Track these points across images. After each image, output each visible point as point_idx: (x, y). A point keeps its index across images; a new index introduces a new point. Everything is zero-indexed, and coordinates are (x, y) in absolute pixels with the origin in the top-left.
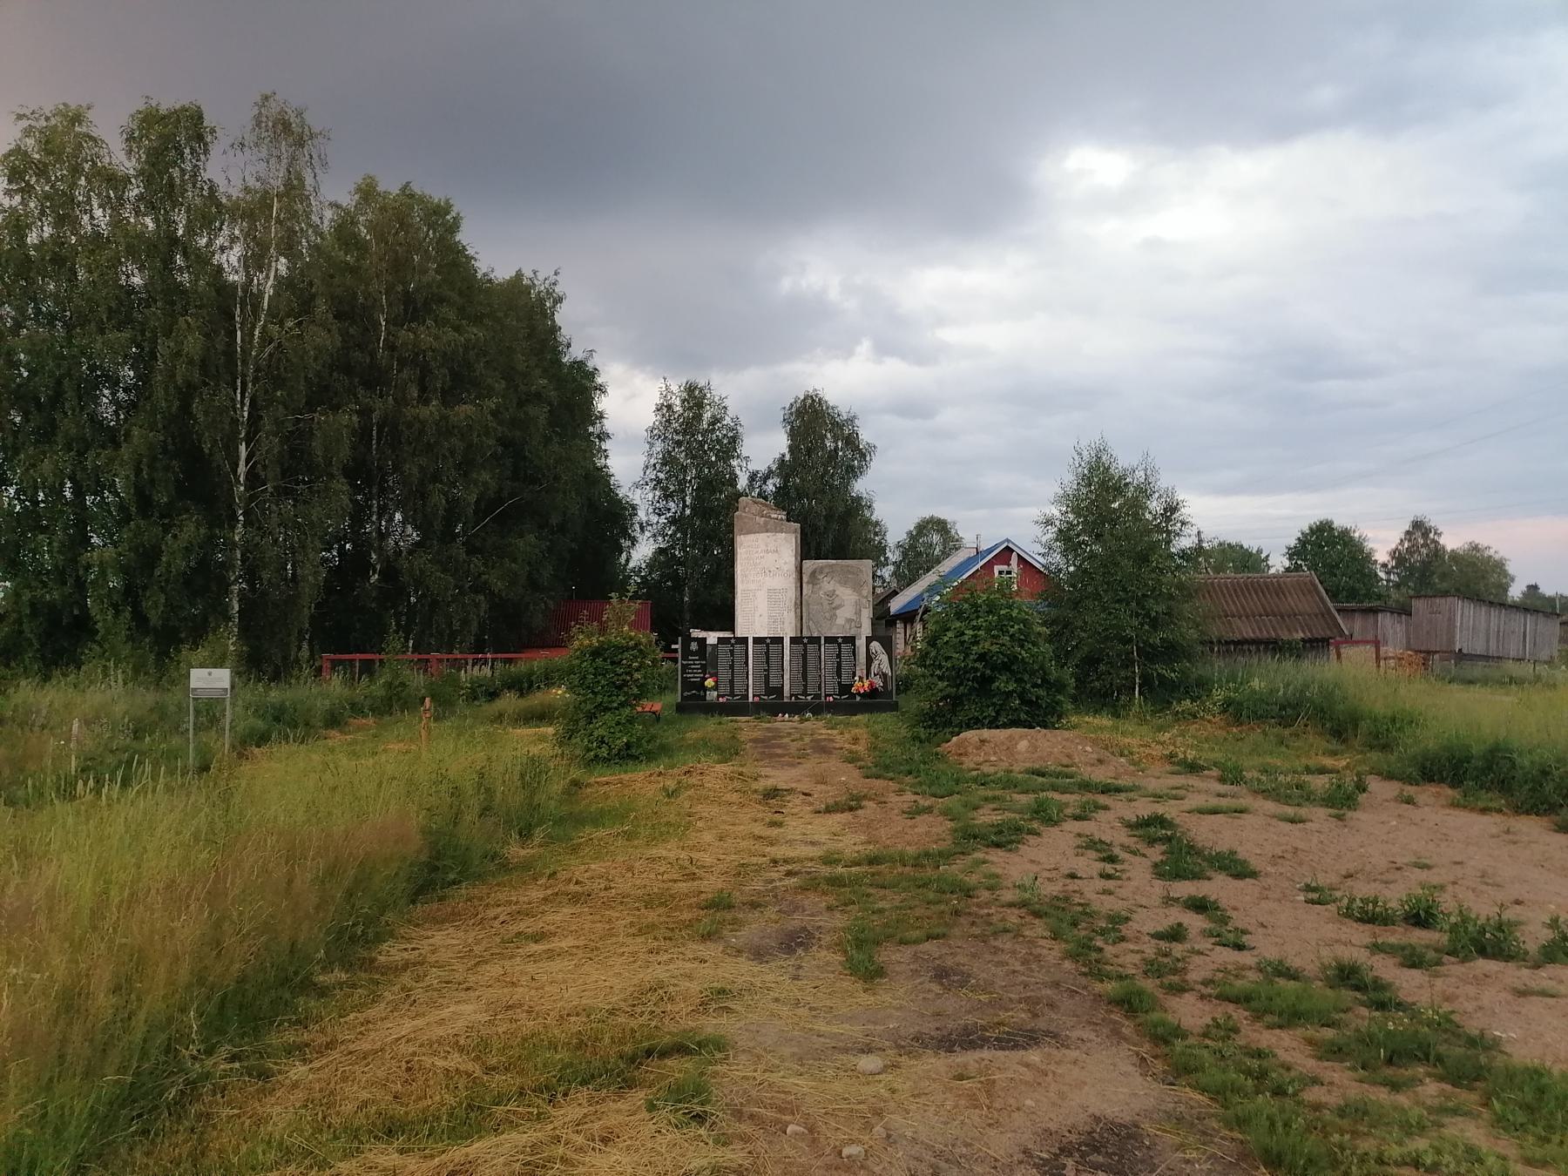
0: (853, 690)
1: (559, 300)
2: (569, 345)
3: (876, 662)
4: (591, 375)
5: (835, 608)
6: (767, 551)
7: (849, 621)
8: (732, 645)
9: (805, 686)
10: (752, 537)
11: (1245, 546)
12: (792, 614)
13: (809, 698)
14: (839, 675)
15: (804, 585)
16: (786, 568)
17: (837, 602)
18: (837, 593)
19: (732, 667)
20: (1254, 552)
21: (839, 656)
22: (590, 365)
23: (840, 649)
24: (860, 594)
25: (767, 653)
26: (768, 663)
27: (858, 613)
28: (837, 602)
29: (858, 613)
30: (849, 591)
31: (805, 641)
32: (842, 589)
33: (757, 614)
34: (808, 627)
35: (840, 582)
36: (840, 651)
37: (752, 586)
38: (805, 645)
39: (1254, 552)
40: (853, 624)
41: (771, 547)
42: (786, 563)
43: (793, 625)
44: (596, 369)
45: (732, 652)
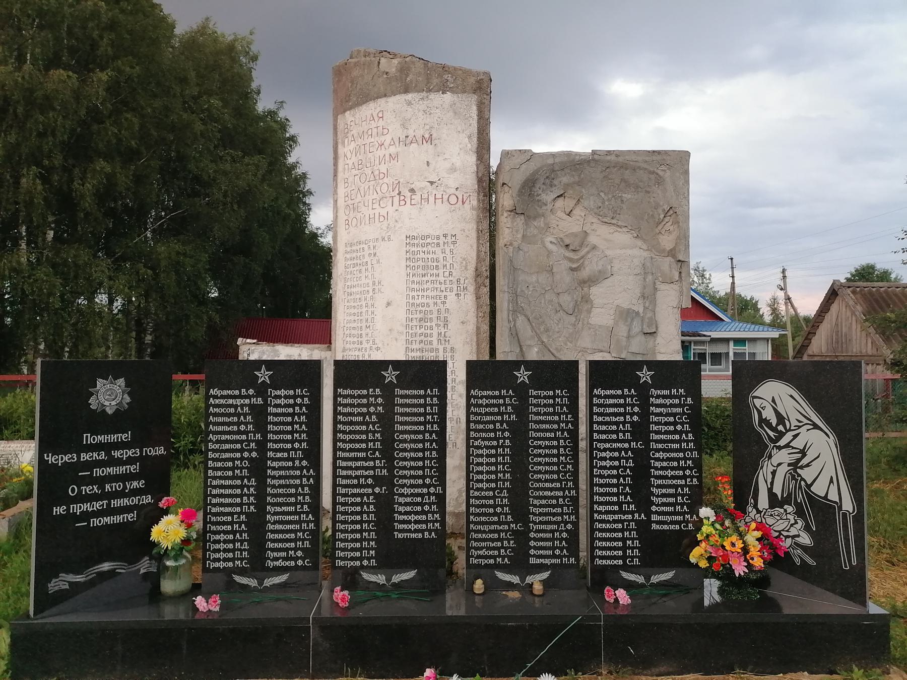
0: (696, 555)
1: (254, 58)
2: (259, 93)
3: (782, 457)
4: (283, 126)
5: (592, 281)
6: (407, 141)
7: (626, 315)
8: (262, 390)
9: (522, 538)
10: (369, 109)
11: (743, 296)
12: (469, 299)
13: (537, 581)
14: (643, 501)
15: (505, 221)
16: (452, 181)
17: (590, 268)
18: (593, 239)
19: (258, 469)
20: (748, 299)
21: (641, 431)
22: (282, 114)
23: (645, 405)
24: (654, 247)
25: (387, 420)
26: (388, 452)
27: (649, 296)
28: (590, 268)
29: (649, 296)
30: (624, 237)
31: (523, 375)
32: (604, 230)
33: (380, 301)
34: (515, 335)
35: (598, 213)
36: (645, 414)
37: (369, 232)
38: (521, 392)
39: (748, 299)
40: (636, 327)
41: (416, 129)
42: (453, 169)
43: (471, 327)
44: (287, 120)
45: (260, 415)
